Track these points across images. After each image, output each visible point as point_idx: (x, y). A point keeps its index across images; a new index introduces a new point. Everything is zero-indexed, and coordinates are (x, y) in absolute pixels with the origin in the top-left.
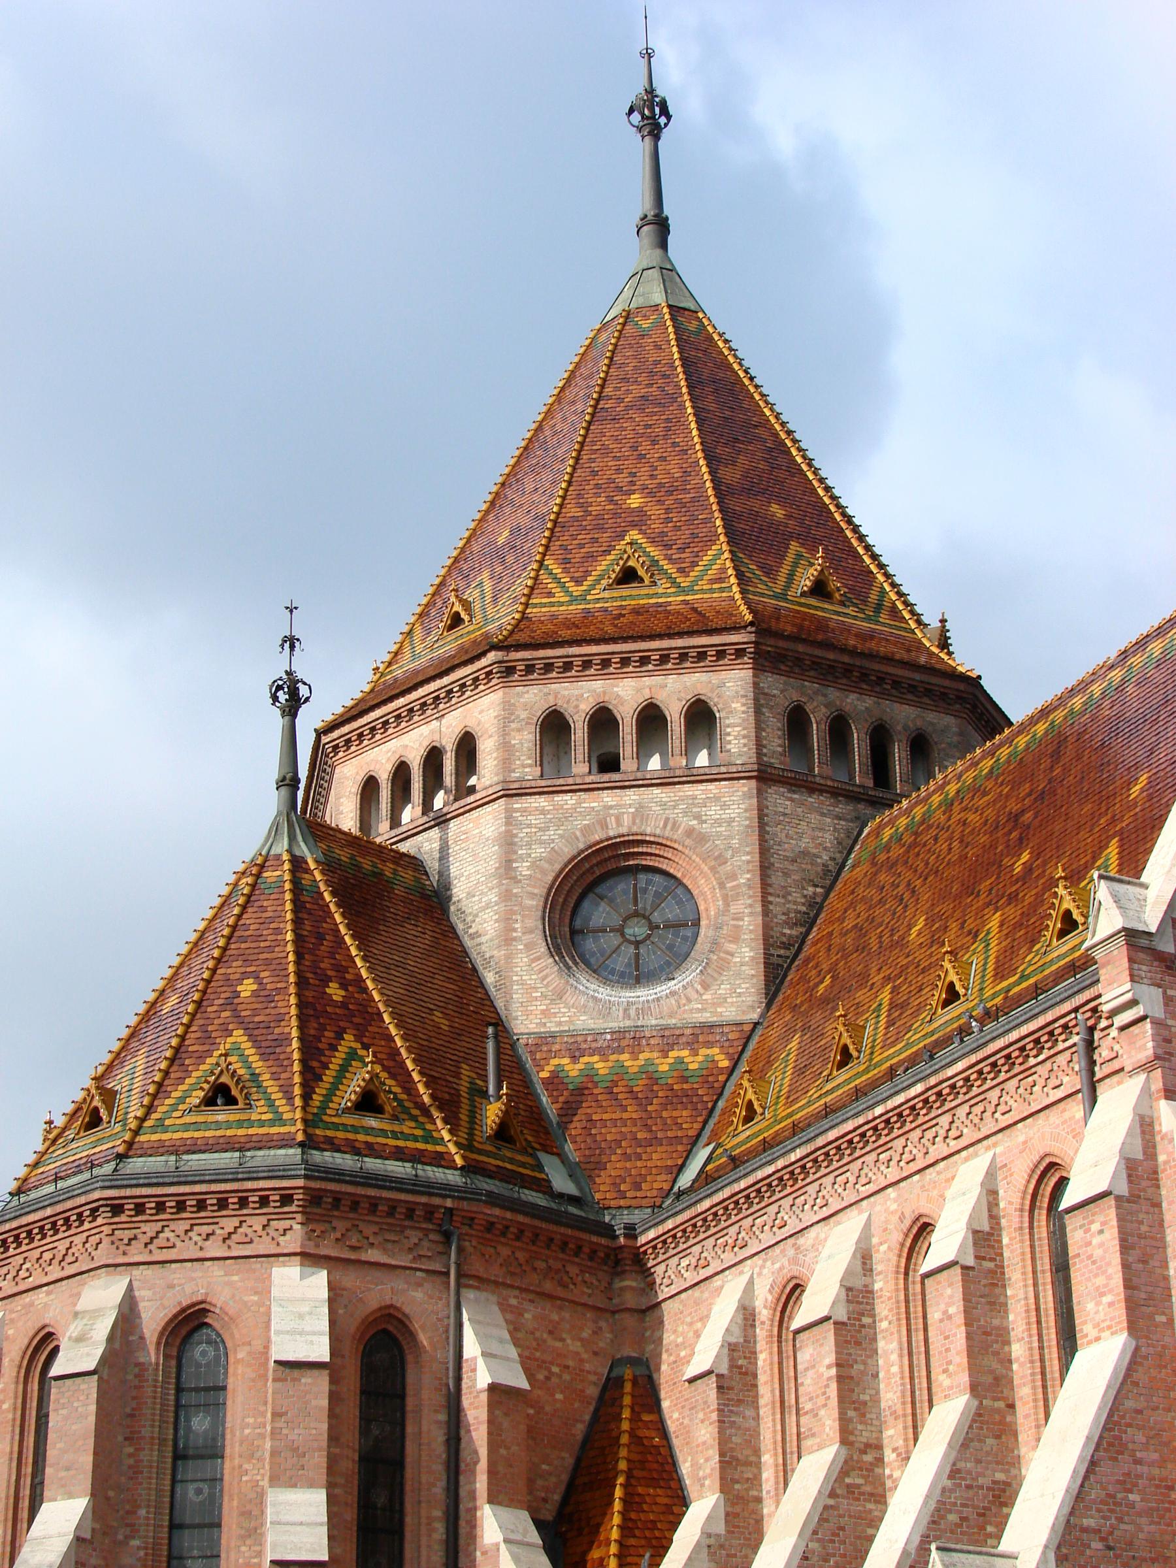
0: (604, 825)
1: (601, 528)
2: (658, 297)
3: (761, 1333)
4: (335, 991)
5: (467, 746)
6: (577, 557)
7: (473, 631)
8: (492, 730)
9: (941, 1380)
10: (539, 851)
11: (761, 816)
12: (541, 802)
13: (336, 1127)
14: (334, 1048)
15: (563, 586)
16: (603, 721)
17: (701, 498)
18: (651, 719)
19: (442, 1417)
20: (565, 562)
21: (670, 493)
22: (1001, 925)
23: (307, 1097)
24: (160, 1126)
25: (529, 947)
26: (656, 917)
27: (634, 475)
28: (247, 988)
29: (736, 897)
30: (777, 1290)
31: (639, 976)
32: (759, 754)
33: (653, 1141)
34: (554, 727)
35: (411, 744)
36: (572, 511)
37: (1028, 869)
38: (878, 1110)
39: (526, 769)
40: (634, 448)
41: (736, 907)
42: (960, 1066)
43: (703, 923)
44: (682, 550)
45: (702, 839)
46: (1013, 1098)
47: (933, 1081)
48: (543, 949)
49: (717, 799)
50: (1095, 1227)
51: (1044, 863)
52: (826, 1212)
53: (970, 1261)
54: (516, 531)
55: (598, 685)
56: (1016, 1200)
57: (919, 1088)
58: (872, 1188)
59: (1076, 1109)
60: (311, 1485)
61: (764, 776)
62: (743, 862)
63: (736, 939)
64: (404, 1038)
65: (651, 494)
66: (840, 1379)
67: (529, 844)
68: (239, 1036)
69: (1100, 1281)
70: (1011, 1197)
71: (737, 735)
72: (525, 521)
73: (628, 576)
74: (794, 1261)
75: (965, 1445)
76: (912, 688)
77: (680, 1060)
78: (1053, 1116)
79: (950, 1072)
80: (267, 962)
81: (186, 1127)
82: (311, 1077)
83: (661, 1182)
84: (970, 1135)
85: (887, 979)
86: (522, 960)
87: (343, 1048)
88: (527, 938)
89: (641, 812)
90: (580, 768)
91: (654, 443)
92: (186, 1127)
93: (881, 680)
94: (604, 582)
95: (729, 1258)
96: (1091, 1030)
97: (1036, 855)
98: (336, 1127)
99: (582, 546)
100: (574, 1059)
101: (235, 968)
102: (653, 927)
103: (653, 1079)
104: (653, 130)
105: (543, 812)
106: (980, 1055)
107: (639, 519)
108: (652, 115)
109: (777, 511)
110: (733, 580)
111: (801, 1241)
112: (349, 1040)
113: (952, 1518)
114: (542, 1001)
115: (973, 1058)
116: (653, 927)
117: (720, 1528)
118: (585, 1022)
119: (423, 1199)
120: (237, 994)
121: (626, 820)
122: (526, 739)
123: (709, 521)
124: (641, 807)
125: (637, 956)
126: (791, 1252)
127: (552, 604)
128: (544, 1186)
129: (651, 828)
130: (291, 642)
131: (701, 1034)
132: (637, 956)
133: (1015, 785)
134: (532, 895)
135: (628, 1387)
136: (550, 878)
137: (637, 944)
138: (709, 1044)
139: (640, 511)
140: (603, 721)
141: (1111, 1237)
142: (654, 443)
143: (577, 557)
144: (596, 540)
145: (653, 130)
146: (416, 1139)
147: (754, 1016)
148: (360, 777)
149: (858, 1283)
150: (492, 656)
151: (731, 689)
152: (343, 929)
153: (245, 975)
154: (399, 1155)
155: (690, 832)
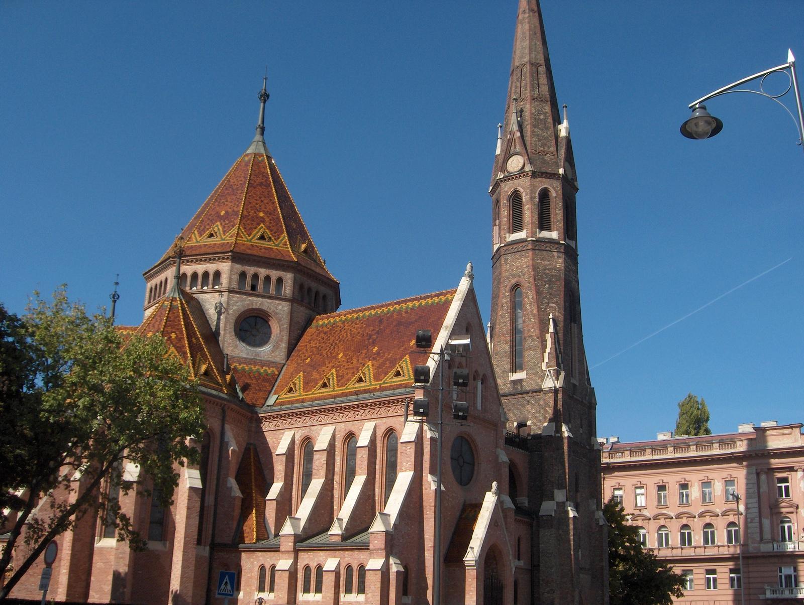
0: (253, 305)
1: (253, 220)
2: (262, 151)
3: (296, 447)
5: (217, 274)
6: (248, 227)
7: (216, 241)
8: (227, 273)
9: (358, 470)
10: (235, 308)
11: (291, 311)
15: (245, 235)
17: (278, 218)
20: (245, 228)
21: (270, 214)
22: (373, 365)
25: (230, 332)
27: (260, 206)
28: (173, 336)
29: (283, 331)
30: (302, 438)
32: (293, 295)
33: (260, 390)
34: (243, 275)
35: (200, 268)
36: (245, 213)
37: (378, 353)
38: (343, 405)
39: (235, 286)
40: (260, 198)
41: (283, 333)
42: (370, 401)
43: (273, 335)
44: (275, 233)
45: (276, 314)
46: (383, 411)
47: (361, 402)
48: (233, 334)
49: (281, 304)
50: (409, 447)
51: (384, 353)
52: (320, 423)
53: (370, 446)
54: (227, 212)
56: (381, 434)
57: (357, 403)
58: (337, 421)
59: (402, 419)
61: (292, 301)
62: (286, 321)
63: (281, 341)
64: (210, 356)
65: (266, 214)
67: (233, 306)
69: (408, 459)
70: (380, 434)
71: (288, 289)
72: (230, 211)
73: (262, 238)
74: (310, 432)
76: (325, 284)
77: (266, 370)
79: (367, 402)
80: (178, 329)
83: (262, 401)
84: (368, 416)
85: (333, 367)
86: (228, 335)
88: (230, 330)
89: (262, 303)
90: (248, 287)
91: (265, 198)
93: (320, 280)
94: (256, 237)
95: (287, 426)
96: (409, 403)
97: (380, 349)
99: (249, 225)
100: (240, 365)
101: (169, 329)
103: (259, 374)
105: (237, 298)
106: (377, 400)
107: (263, 220)
110: (289, 246)
111: (312, 428)
113: (361, 501)
114: (233, 347)
115: (375, 400)
117: (283, 490)
118: (244, 355)
121: (258, 305)
122: (236, 277)
123: (281, 226)
124: (262, 302)
126: (308, 430)
127: (243, 241)
129: (264, 308)
131: (269, 364)
134: (232, 319)
135: (252, 451)
136: (237, 315)
138: (273, 367)
139: (262, 218)
141: (413, 450)
142: (265, 198)
143: (248, 227)
144: (252, 224)
147: (284, 362)
149: (332, 442)
150: (230, 254)
151: (289, 278)
153: (172, 332)
155: (274, 311)
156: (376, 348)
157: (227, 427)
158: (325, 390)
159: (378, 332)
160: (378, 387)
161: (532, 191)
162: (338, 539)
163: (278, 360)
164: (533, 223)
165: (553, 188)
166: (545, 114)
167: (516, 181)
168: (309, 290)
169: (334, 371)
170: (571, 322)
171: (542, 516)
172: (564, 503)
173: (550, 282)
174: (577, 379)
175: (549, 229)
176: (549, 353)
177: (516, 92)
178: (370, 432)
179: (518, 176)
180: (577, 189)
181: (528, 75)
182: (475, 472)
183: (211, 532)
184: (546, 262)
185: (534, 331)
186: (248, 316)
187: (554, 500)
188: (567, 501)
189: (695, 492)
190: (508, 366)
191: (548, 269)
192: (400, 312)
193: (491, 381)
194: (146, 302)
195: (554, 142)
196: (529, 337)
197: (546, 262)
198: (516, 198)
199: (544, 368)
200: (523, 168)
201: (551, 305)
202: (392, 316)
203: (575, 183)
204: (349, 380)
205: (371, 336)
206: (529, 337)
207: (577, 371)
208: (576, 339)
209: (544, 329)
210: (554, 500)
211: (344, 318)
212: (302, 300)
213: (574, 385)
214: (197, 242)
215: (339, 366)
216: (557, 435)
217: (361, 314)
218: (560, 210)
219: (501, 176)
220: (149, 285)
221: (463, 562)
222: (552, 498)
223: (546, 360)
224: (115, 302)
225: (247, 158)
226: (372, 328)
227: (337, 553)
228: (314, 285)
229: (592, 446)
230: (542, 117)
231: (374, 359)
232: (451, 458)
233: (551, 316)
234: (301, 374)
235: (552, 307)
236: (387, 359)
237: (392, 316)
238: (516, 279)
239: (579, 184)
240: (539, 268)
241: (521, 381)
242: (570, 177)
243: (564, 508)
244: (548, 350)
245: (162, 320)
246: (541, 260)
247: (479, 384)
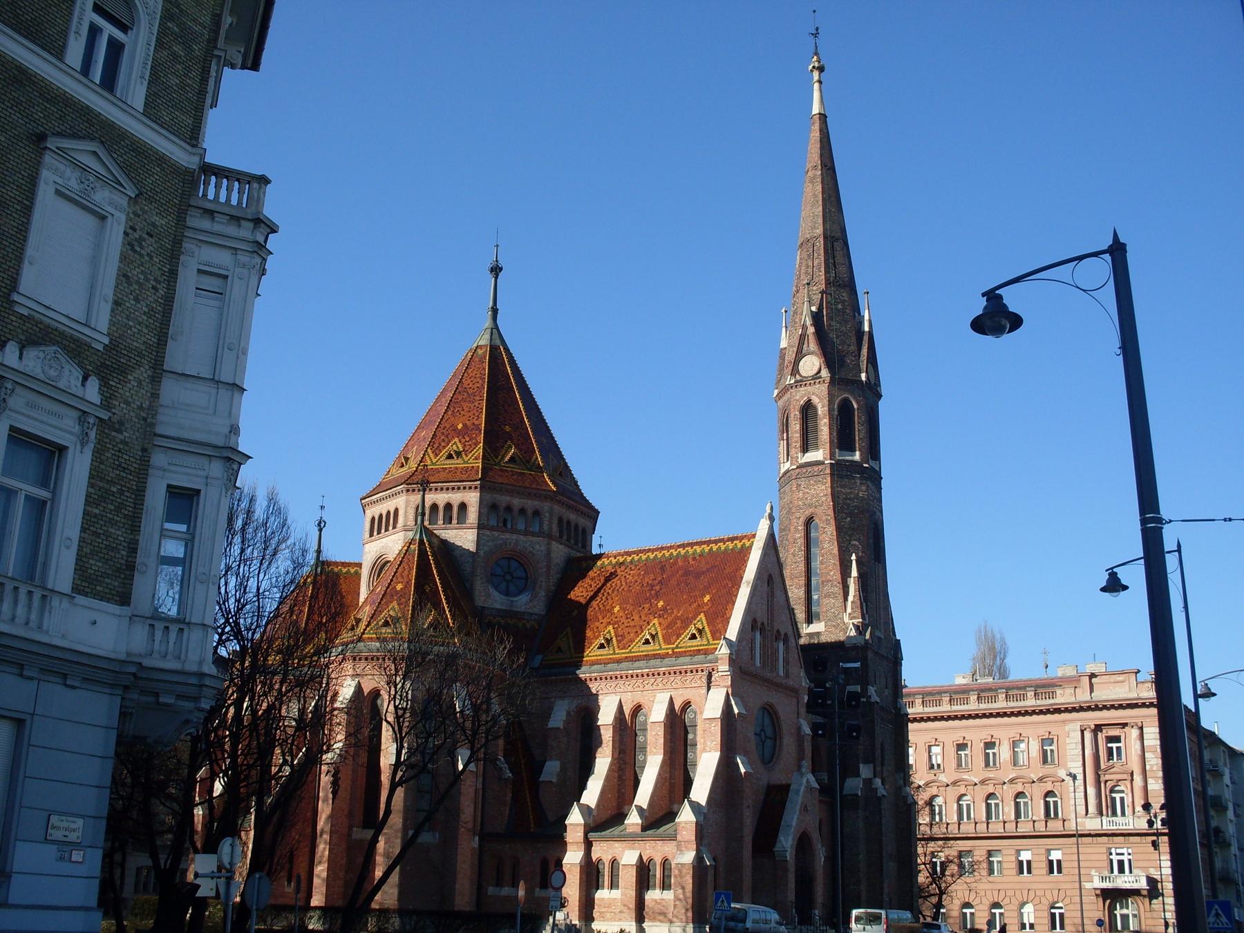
5: (463, 507)
10: (486, 548)
12: (488, 533)
18: (522, 511)
37: (664, 609)
54: (465, 425)
59: (704, 690)
78: (694, 690)
85: (609, 623)
97: (667, 603)
108: (496, 270)
133: (647, 573)
140: (509, 509)
156: (661, 604)
158: (602, 651)
159: (660, 582)
160: (670, 652)
161: (831, 402)
162: (639, 829)
163: (536, 610)
164: (831, 442)
166: (843, 302)
167: (809, 388)
168: (569, 522)
169: (610, 628)
173: (851, 514)
177: (806, 273)
178: (665, 705)
180: (880, 396)
181: (822, 252)
185: (835, 575)
189: (1004, 753)
192: (685, 557)
194: (367, 535)
195: (854, 339)
196: (828, 581)
198: (808, 410)
199: (846, 619)
200: (819, 371)
202: (675, 563)
204: (632, 641)
205: (652, 586)
206: (828, 581)
209: (845, 573)
211: (614, 561)
212: (561, 537)
213: (879, 639)
214: (433, 464)
215: (616, 623)
217: (636, 558)
219: (790, 380)
220: (370, 513)
222: (858, 775)
223: (849, 610)
224: (320, 530)
225: (480, 352)
226: (652, 577)
227: (636, 844)
228: (573, 517)
230: (840, 306)
231: (660, 616)
233: (854, 557)
234: (569, 630)
236: (677, 618)
237: (675, 563)
239: (884, 389)
241: (818, 634)
242: (873, 382)
244: (850, 598)
245: (411, 569)
247: (781, 644)
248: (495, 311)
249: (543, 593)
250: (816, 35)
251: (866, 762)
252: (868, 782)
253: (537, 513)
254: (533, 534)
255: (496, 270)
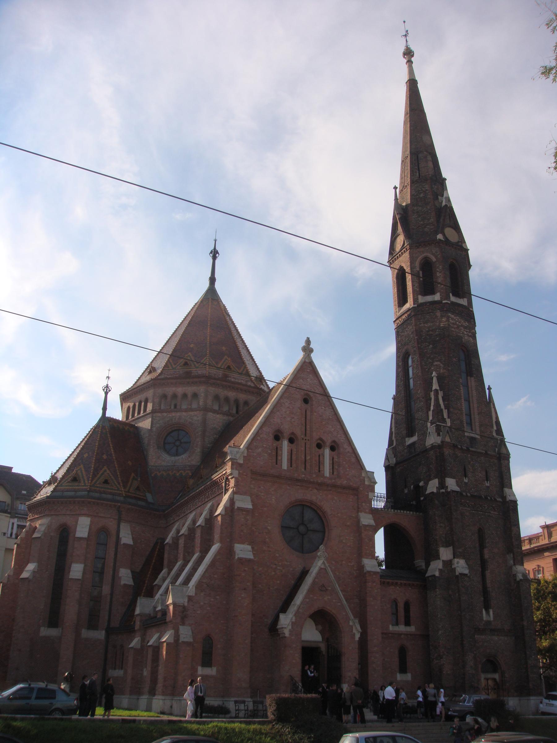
4: (105, 457)
12: (159, 414)
13: (97, 487)
14: (101, 469)
16: (175, 396)
18: (185, 396)
19: (114, 549)
23: (92, 481)
24: (61, 485)
26: (182, 441)
31: (177, 454)
55: (174, 389)
60: (81, 563)
66: (184, 547)
68: (82, 466)
75: (197, 563)
81: (66, 486)
82: (94, 475)
87: (103, 469)
92: (66, 486)
98: (97, 487)
102: (181, 443)
104: (214, 258)
108: (215, 254)
109: (224, 348)
112: (105, 467)
116: (181, 443)
119: (113, 503)
120: (83, 457)
125: (177, 449)
128: (146, 501)
130: (108, 377)
132: (177, 449)
137: (177, 447)
140: (175, 396)
145: (214, 258)
146: (115, 490)
148: (127, 406)
152: (110, 443)
154: (110, 493)
157: (122, 525)
163: (194, 463)
165: (433, 254)
168: (227, 399)
170: (467, 376)
171: (428, 577)
172: (451, 561)
174: (478, 432)
175: (433, 293)
176: (433, 411)
179: (400, 253)
182: (326, 539)
183: (107, 618)
184: (429, 324)
186: (170, 430)
187: (439, 559)
188: (454, 558)
190: (404, 432)
191: (432, 331)
193: (346, 446)
197: (429, 324)
201: (436, 363)
203: (463, 245)
207: (477, 424)
208: (474, 392)
210: (439, 559)
216: (443, 491)
218: (440, 272)
221: (277, 630)
222: (437, 557)
223: (431, 418)
229: (504, 497)
232: (282, 527)
233: (434, 374)
235: (436, 365)
238: (405, 348)
240: (422, 331)
243: (451, 567)
246: (424, 323)
248: (212, 280)
249: (198, 450)
250: (406, 36)
251: (447, 545)
252: (448, 564)
253: (195, 395)
254: (192, 410)
255: (215, 254)
